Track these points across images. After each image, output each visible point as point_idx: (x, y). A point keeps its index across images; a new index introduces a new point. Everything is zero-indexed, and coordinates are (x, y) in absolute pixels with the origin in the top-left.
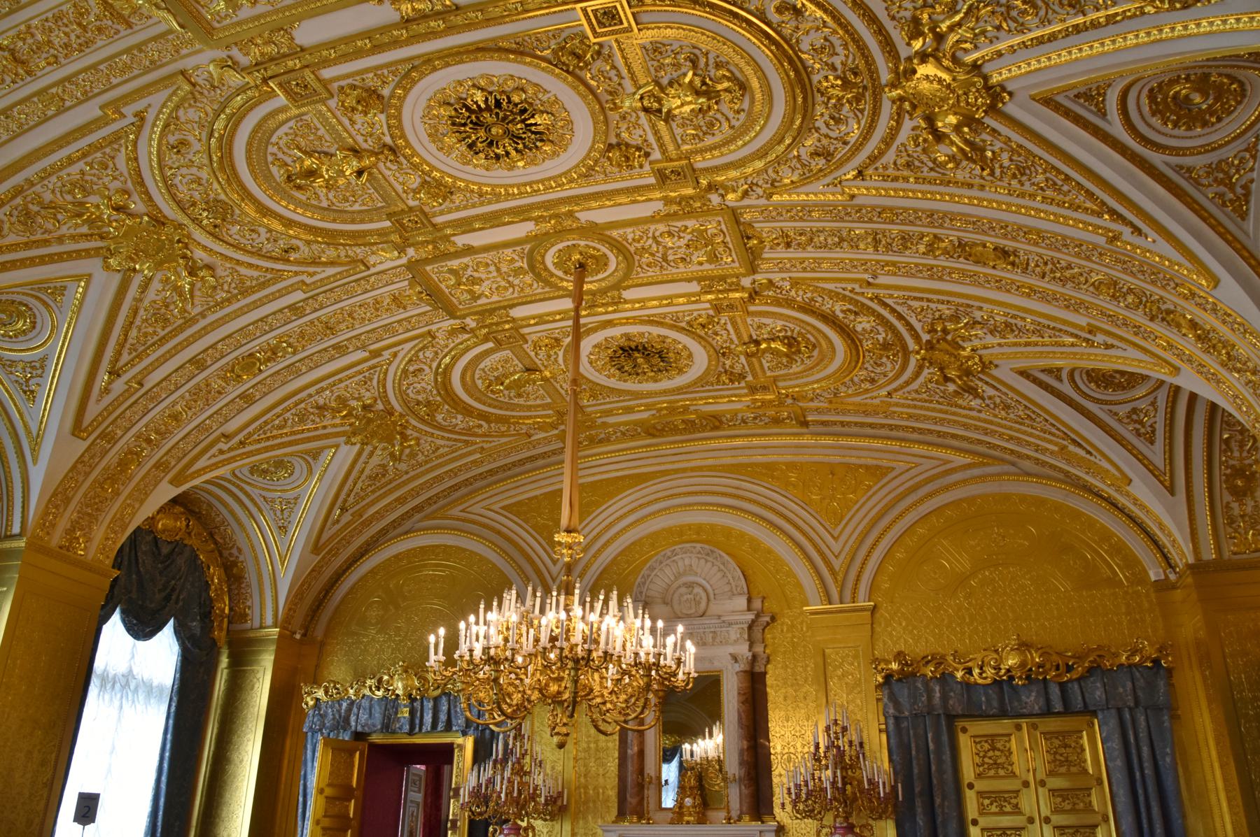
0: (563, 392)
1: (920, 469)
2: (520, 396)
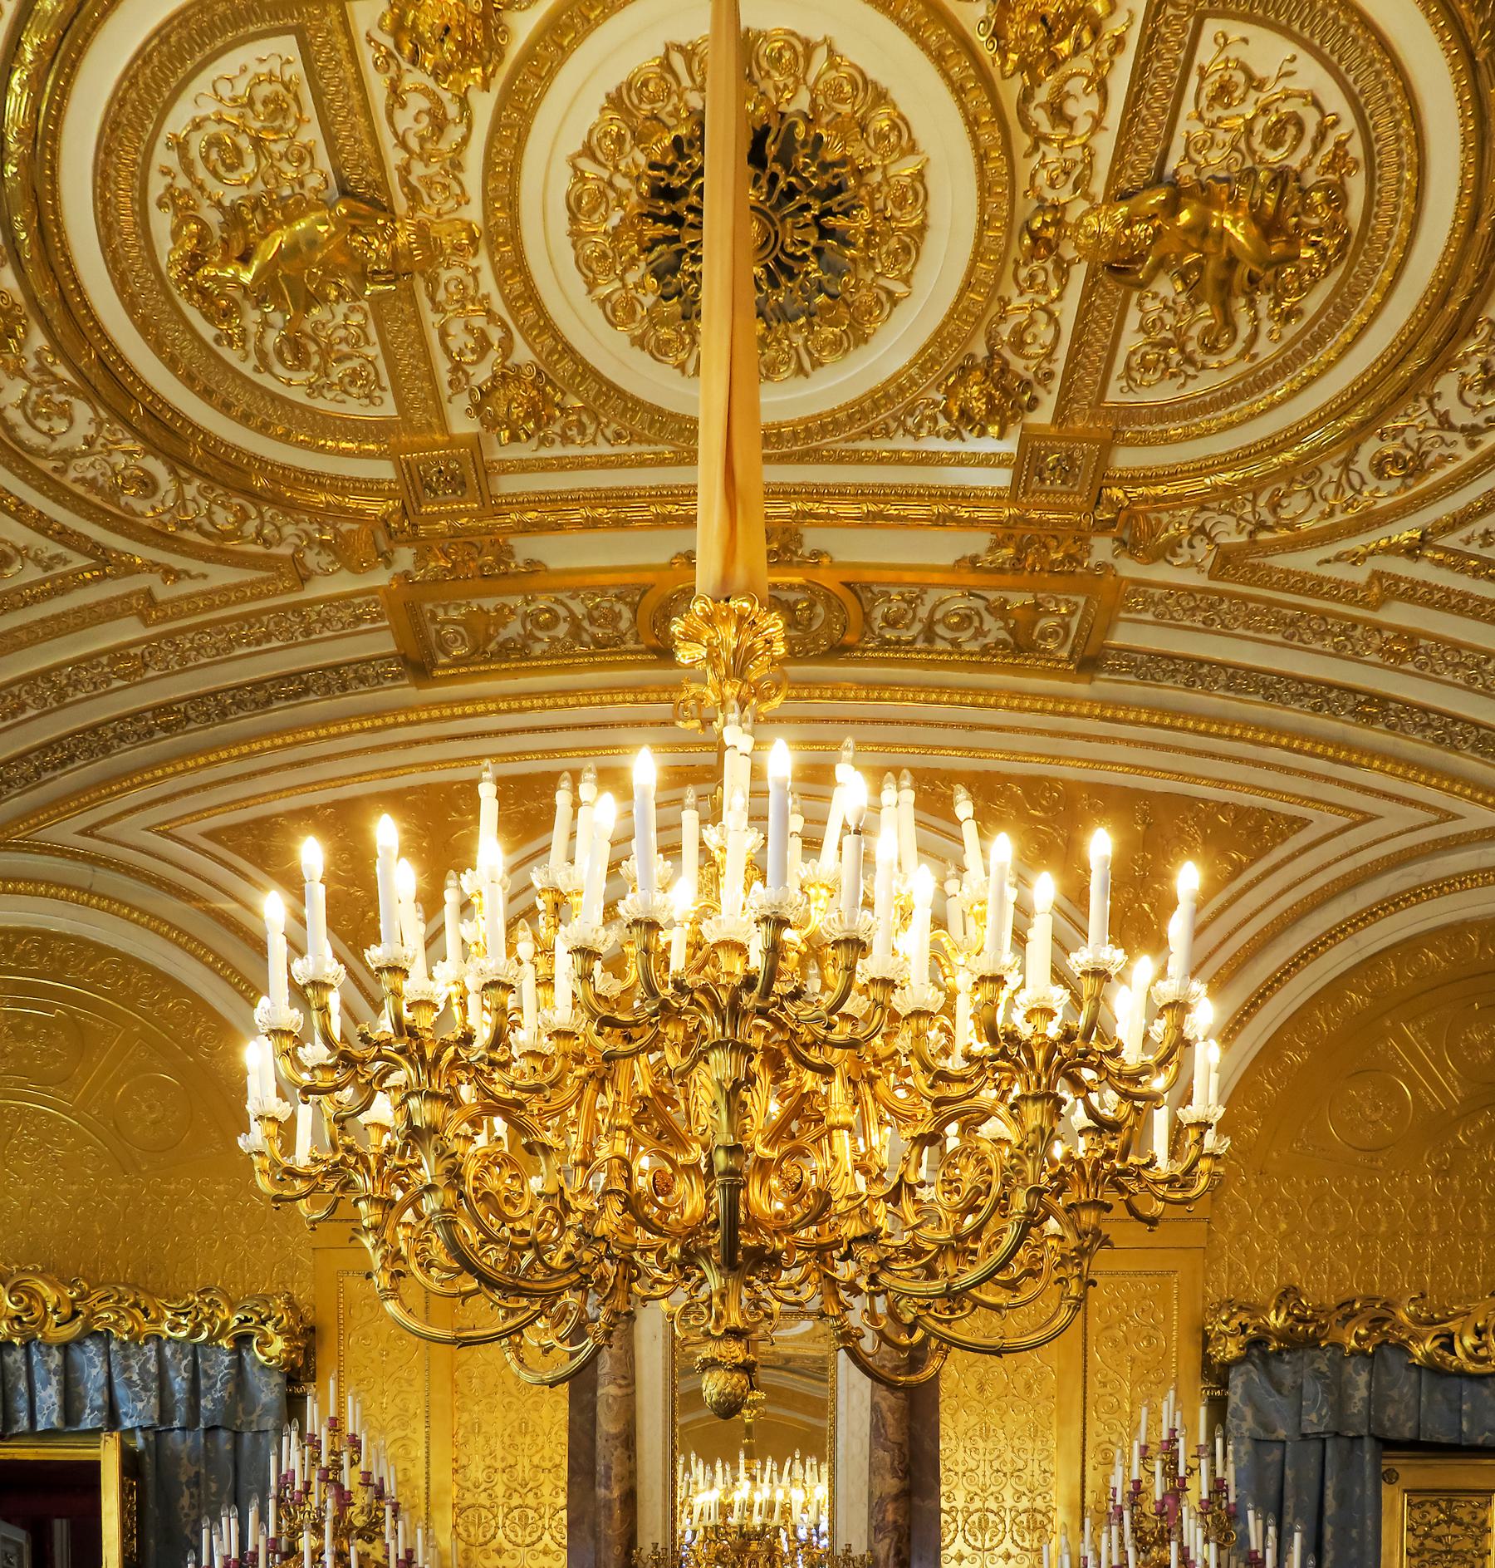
0: (443, 367)
2: (296, 349)
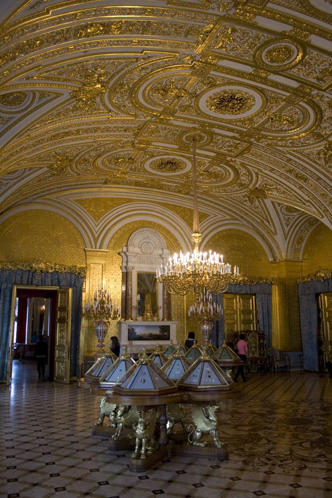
1: (217, 217)
